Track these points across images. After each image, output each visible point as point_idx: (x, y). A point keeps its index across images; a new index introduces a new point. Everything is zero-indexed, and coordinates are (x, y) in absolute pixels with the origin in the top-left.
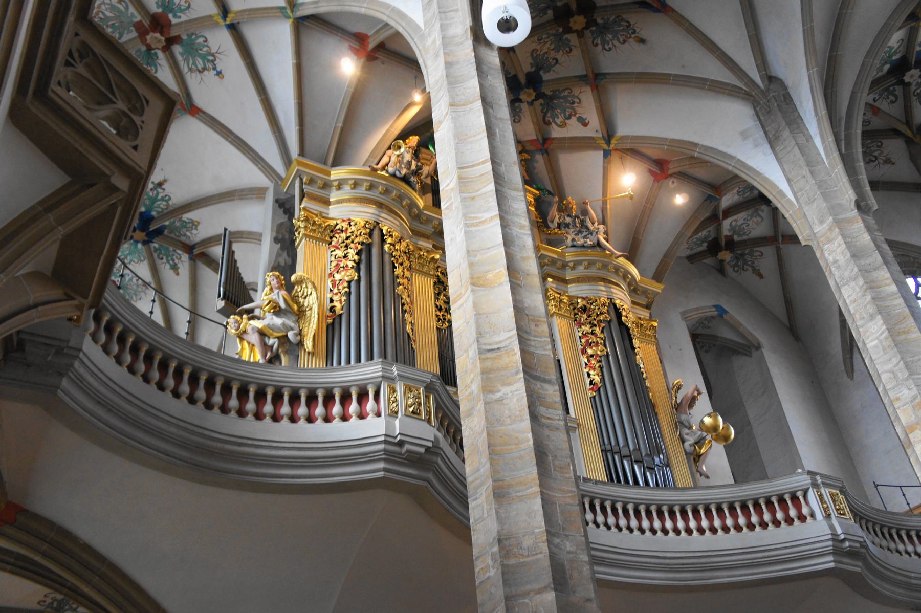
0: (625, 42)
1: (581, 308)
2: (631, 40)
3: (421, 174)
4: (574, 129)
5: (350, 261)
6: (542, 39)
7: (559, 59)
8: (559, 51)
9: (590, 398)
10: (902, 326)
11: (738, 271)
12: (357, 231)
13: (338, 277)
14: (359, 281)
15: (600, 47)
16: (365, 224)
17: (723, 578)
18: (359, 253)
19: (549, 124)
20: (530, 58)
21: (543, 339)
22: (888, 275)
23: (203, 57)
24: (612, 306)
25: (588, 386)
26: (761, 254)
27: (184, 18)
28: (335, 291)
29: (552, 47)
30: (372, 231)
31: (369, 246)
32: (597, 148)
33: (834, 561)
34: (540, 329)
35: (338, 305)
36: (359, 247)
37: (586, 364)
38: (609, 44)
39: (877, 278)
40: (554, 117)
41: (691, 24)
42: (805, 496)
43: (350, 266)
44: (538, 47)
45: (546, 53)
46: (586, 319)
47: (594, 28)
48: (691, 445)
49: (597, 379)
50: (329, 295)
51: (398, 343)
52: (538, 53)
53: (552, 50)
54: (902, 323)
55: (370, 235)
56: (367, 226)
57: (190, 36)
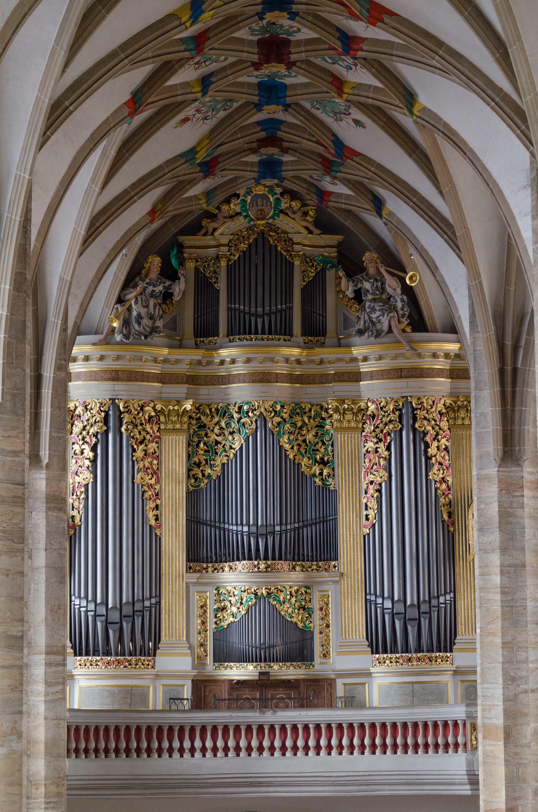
1: (370, 415)
3: (172, 294)
5: (86, 459)
9: (364, 537)
10: (493, 626)
12: (93, 417)
16: (100, 408)
17: (385, 791)
18: (94, 449)
21: (39, 800)
22: (498, 563)
30: (107, 413)
33: (471, 790)
34: (38, 792)
37: (366, 493)
39: (491, 562)
41: (380, 167)
42: (464, 725)
46: (374, 431)
49: (372, 514)
54: (494, 623)
55: (106, 421)
56: (102, 409)
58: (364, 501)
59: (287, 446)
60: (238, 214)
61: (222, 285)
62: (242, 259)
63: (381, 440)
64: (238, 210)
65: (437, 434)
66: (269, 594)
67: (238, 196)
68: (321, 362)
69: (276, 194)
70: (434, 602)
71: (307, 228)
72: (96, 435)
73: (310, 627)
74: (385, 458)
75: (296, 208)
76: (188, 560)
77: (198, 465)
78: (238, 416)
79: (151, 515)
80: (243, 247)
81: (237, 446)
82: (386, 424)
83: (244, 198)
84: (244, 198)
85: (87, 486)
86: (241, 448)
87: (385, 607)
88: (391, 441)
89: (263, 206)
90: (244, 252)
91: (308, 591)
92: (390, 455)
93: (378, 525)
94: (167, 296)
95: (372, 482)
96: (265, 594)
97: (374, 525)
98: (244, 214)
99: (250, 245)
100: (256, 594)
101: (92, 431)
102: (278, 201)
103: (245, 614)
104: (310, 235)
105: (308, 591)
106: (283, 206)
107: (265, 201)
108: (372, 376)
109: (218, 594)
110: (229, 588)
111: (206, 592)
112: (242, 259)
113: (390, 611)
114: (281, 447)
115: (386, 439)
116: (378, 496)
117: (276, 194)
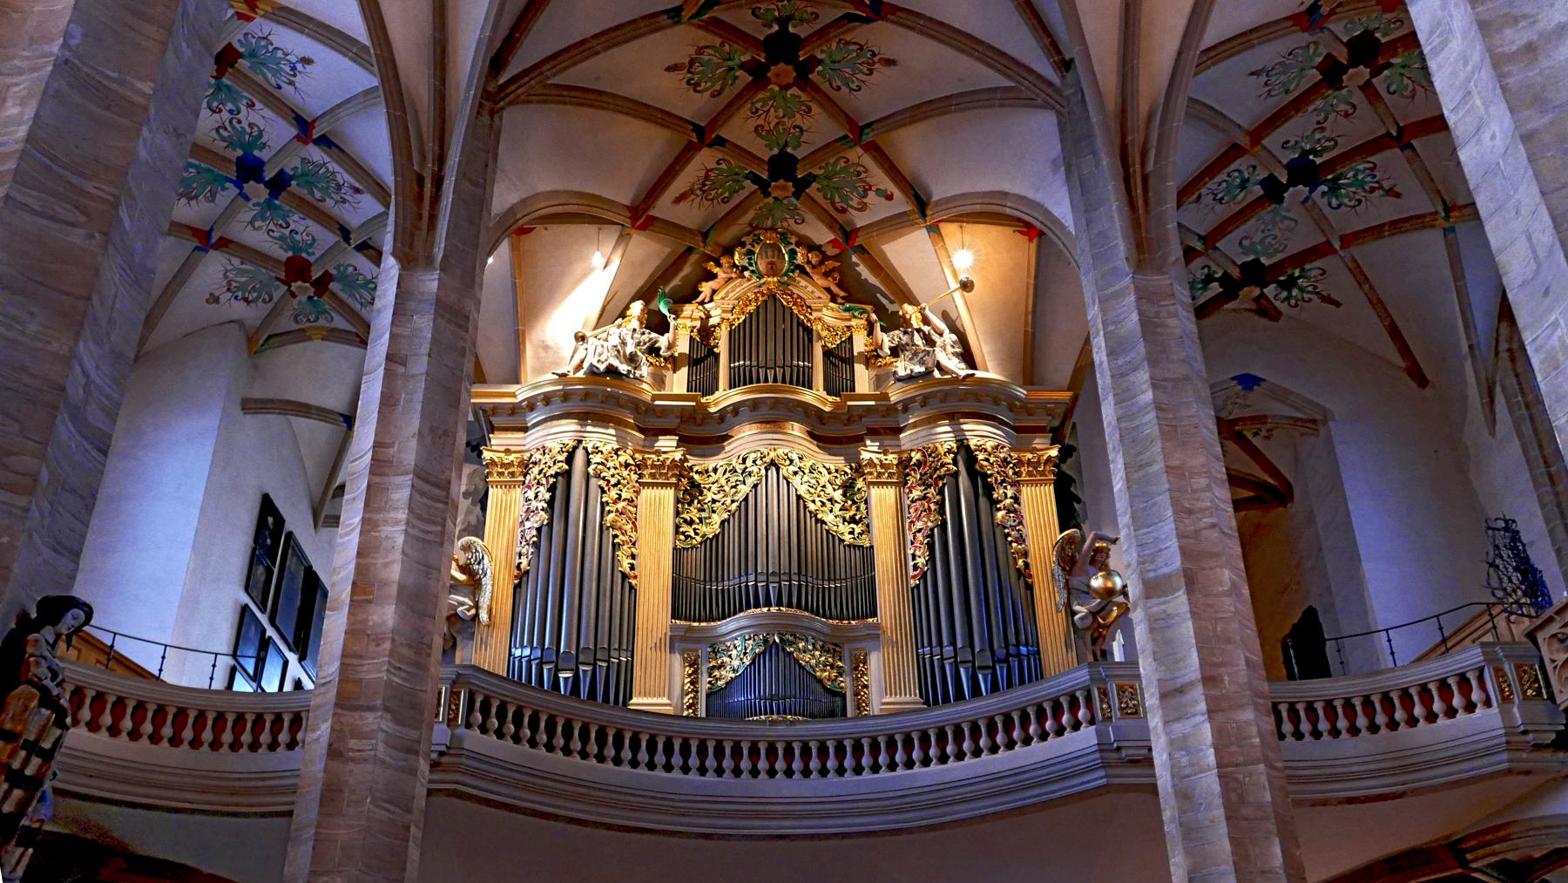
0: (871, 72)
1: (915, 465)
2: (876, 66)
3: (659, 349)
4: (879, 209)
6: (757, 110)
7: (802, 125)
8: (794, 116)
9: (912, 589)
11: (1296, 305)
13: (528, 524)
14: (550, 524)
15: (844, 89)
18: (552, 489)
19: (844, 211)
20: (758, 139)
23: (364, 286)
24: (963, 452)
25: (911, 573)
26: (1321, 272)
27: (318, 253)
28: (524, 543)
29: (781, 113)
31: (568, 475)
32: (913, 225)
35: (524, 561)
36: (552, 480)
37: (912, 543)
38: (853, 82)
40: (845, 199)
43: (540, 508)
44: (760, 122)
45: (778, 123)
46: (920, 479)
47: (820, 68)
48: (1082, 619)
49: (921, 561)
50: (518, 550)
51: (601, 589)
52: (767, 128)
53: (783, 117)
55: (570, 460)
57: (338, 268)
58: (912, 552)
59: (807, 496)
60: (745, 268)
61: (723, 349)
62: (748, 321)
63: (930, 486)
64: (745, 263)
65: (1003, 481)
66: (781, 640)
67: (743, 245)
68: (849, 421)
69: (790, 243)
70: (1012, 650)
71: (828, 290)
72: (556, 475)
73: (842, 688)
74: (937, 503)
75: (814, 261)
76: (673, 617)
77: (691, 523)
78: (743, 466)
79: (625, 564)
80: (752, 308)
81: (740, 497)
82: (936, 469)
83: (749, 247)
84: (749, 247)
85: (539, 530)
86: (746, 499)
87: (945, 657)
88: (944, 485)
89: (773, 257)
90: (751, 314)
91: (838, 649)
92: (944, 499)
93: (931, 575)
94: (653, 350)
95: (920, 531)
96: (777, 641)
97: (924, 575)
98: (751, 268)
99: (758, 307)
100: (766, 641)
101: (552, 472)
102: (793, 254)
103: (750, 665)
104: (831, 304)
105: (838, 649)
106: (800, 259)
107: (776, 253)
108: (914, 425)
109: (713, 651)
110: (728, 644)
111: (697, 650)
112: (748, 321)
113: (952, 660)
114: (799, 497)
115: (937, 484)
116: (928, 543)
117: (790, 243)
